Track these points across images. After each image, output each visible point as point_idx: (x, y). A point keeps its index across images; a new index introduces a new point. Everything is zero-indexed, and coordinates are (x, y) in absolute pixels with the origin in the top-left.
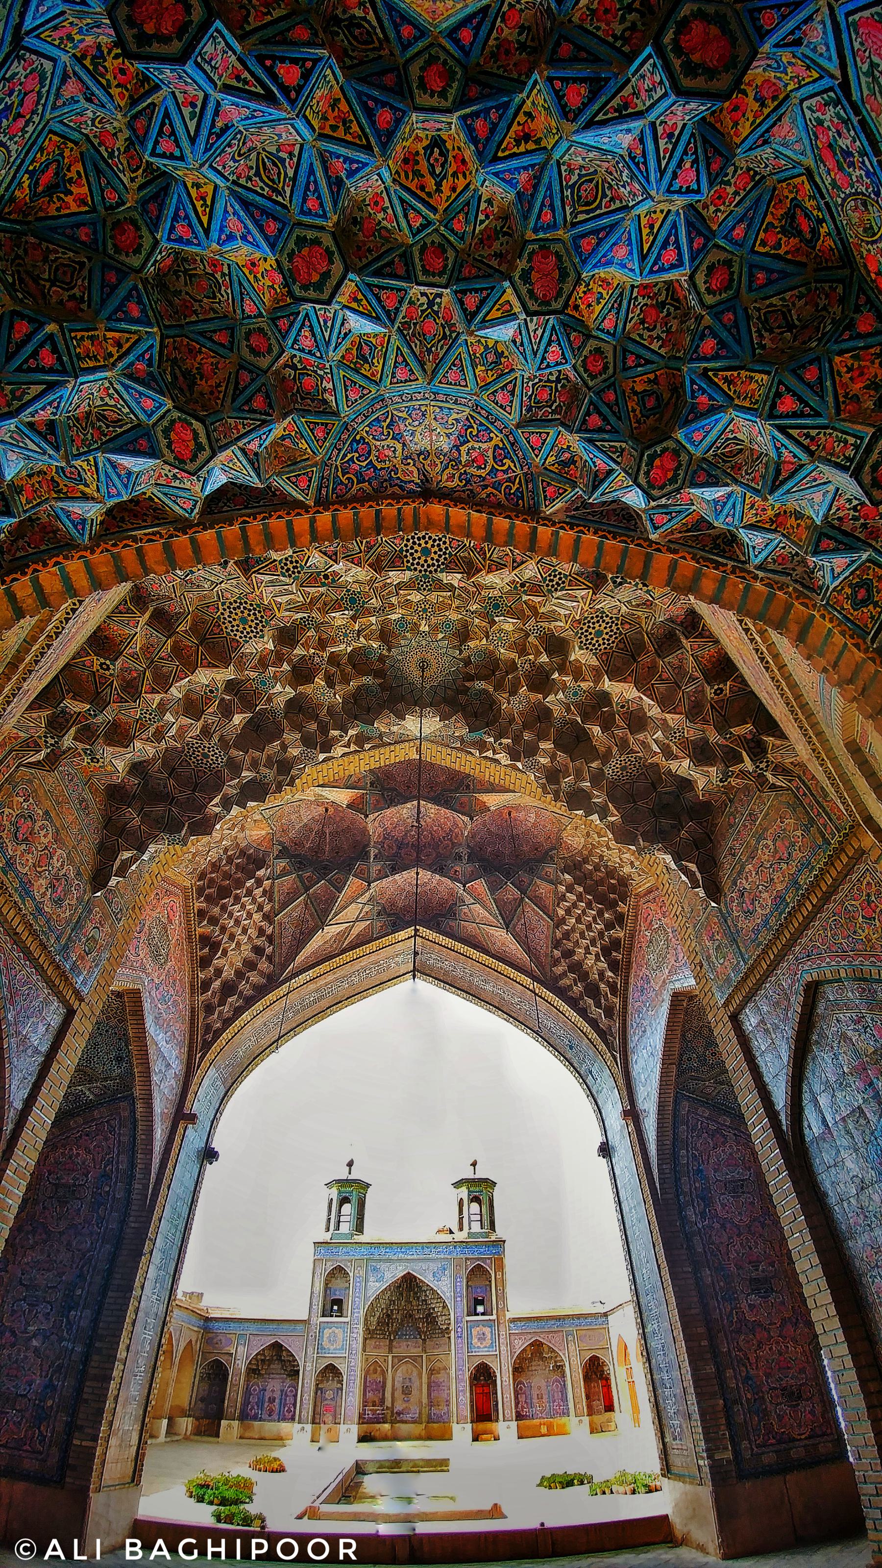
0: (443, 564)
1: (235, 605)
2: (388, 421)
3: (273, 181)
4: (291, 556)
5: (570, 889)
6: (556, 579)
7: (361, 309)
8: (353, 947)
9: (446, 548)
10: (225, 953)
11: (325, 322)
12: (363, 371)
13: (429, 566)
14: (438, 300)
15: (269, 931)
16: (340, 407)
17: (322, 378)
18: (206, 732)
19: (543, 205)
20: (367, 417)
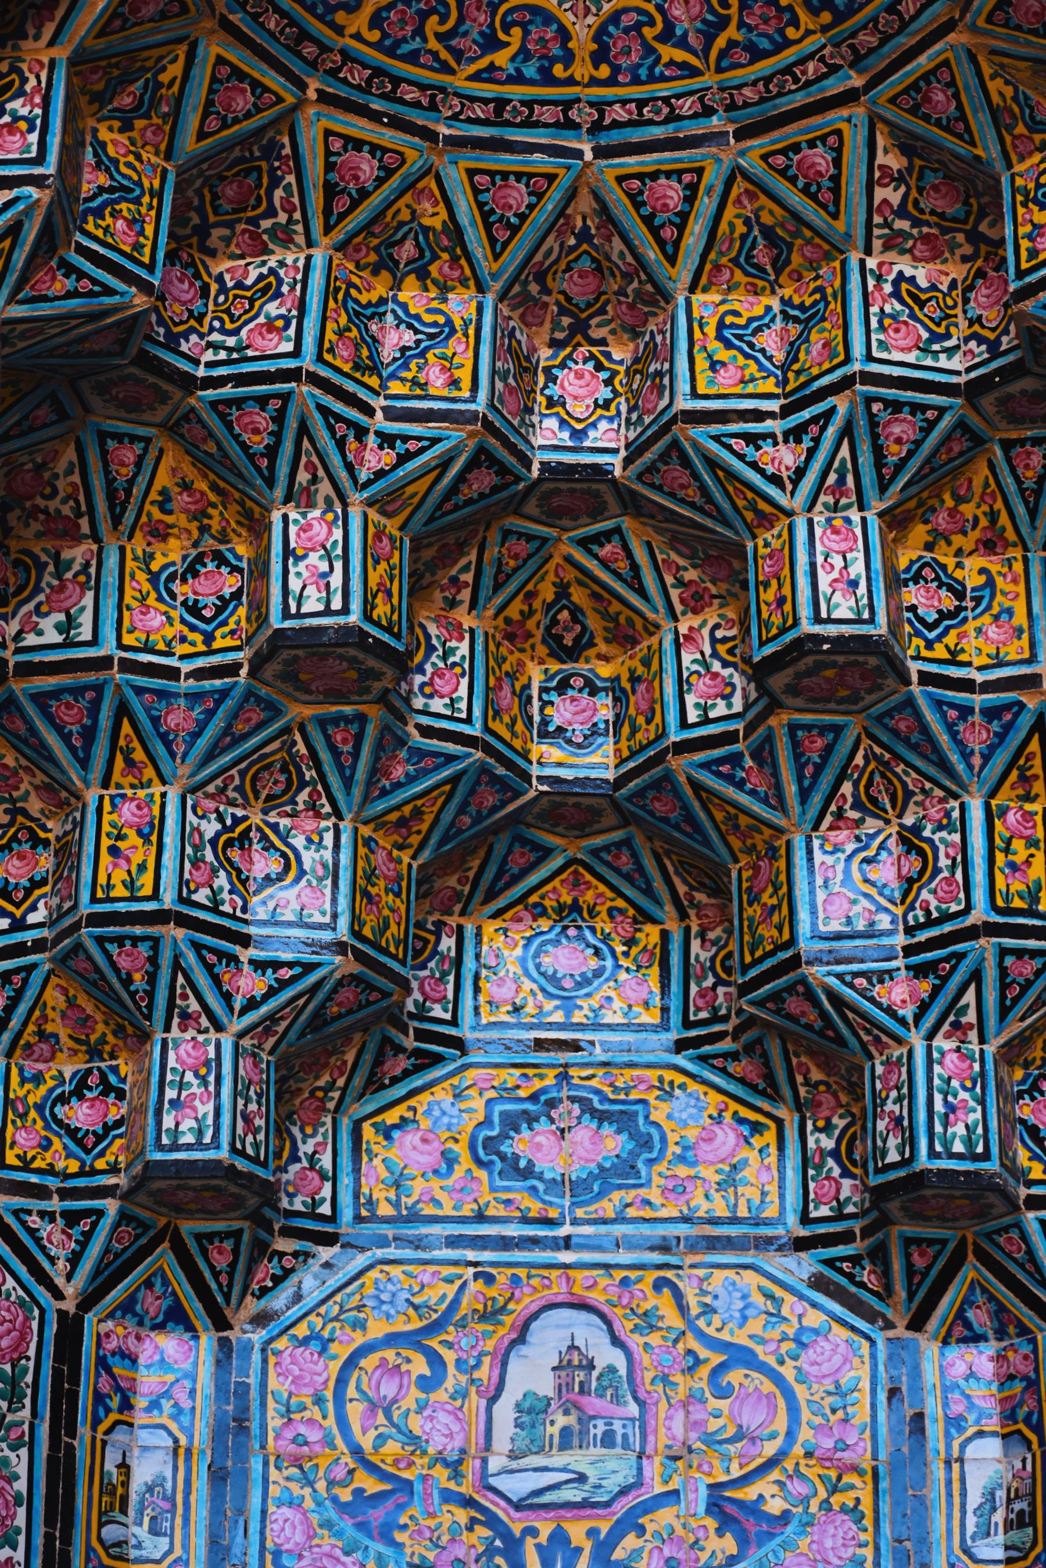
2: (721, 42)
3: (883, 776)
7: (750, 495)
11: (841, 480)
12: (778, 211)
14: (560, 336)
16: (863, 132)
17: (902, 212)
19: (356, 755)
20: (788, 70)
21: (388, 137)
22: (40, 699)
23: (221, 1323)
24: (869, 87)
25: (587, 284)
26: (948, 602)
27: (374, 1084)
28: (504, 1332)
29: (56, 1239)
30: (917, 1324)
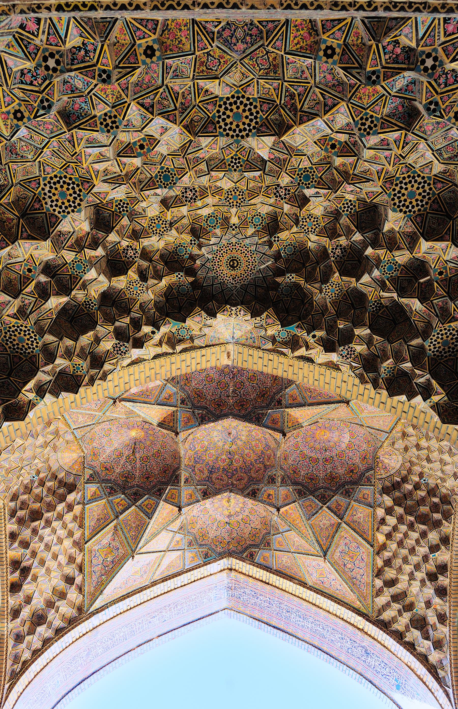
0: (254, 128)
1: (55, 180)
4: (110, 111)
5: (389, 511)
6: (368, 123)
8: (164, 580)
9: (257, 113)
10: (35, 578)
13: (240, 131)
15: (79, 560)
18: (22, 313)
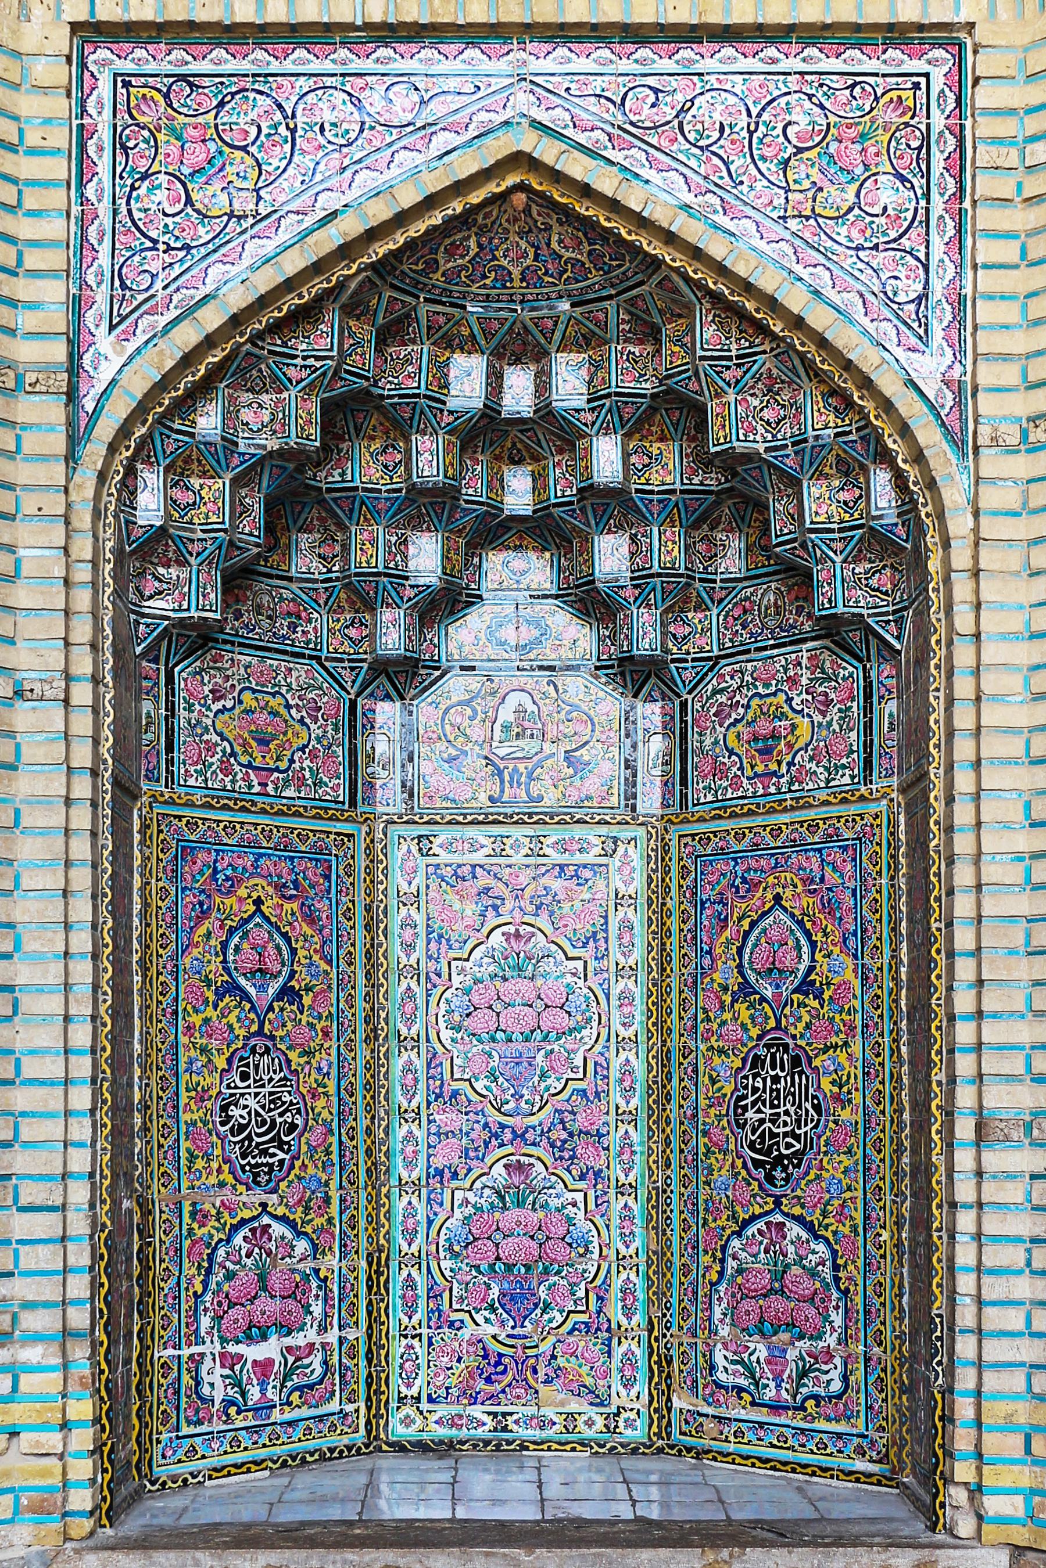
21: (449, 310)
22: (335, 500)
23: (402, 698)
24: (618, 294)
25: (519, 346)
26: (646, 460)
27: (452, 613)
28: (497, 700)
29: (347, 676)
30: (635, 696)
